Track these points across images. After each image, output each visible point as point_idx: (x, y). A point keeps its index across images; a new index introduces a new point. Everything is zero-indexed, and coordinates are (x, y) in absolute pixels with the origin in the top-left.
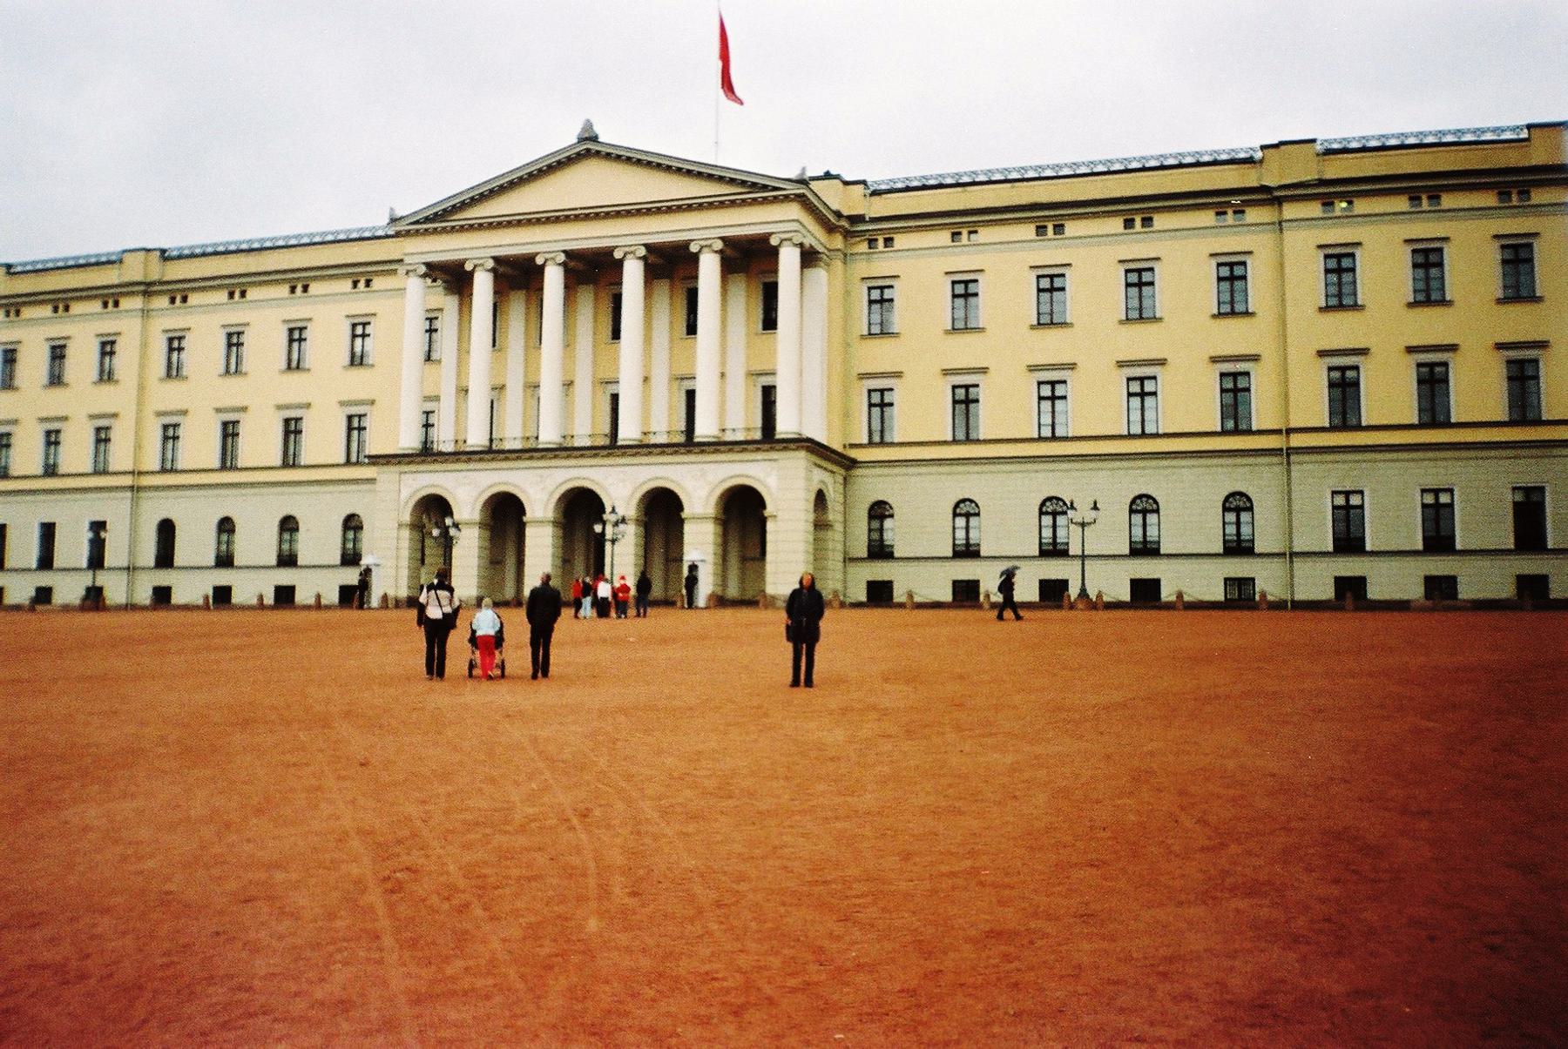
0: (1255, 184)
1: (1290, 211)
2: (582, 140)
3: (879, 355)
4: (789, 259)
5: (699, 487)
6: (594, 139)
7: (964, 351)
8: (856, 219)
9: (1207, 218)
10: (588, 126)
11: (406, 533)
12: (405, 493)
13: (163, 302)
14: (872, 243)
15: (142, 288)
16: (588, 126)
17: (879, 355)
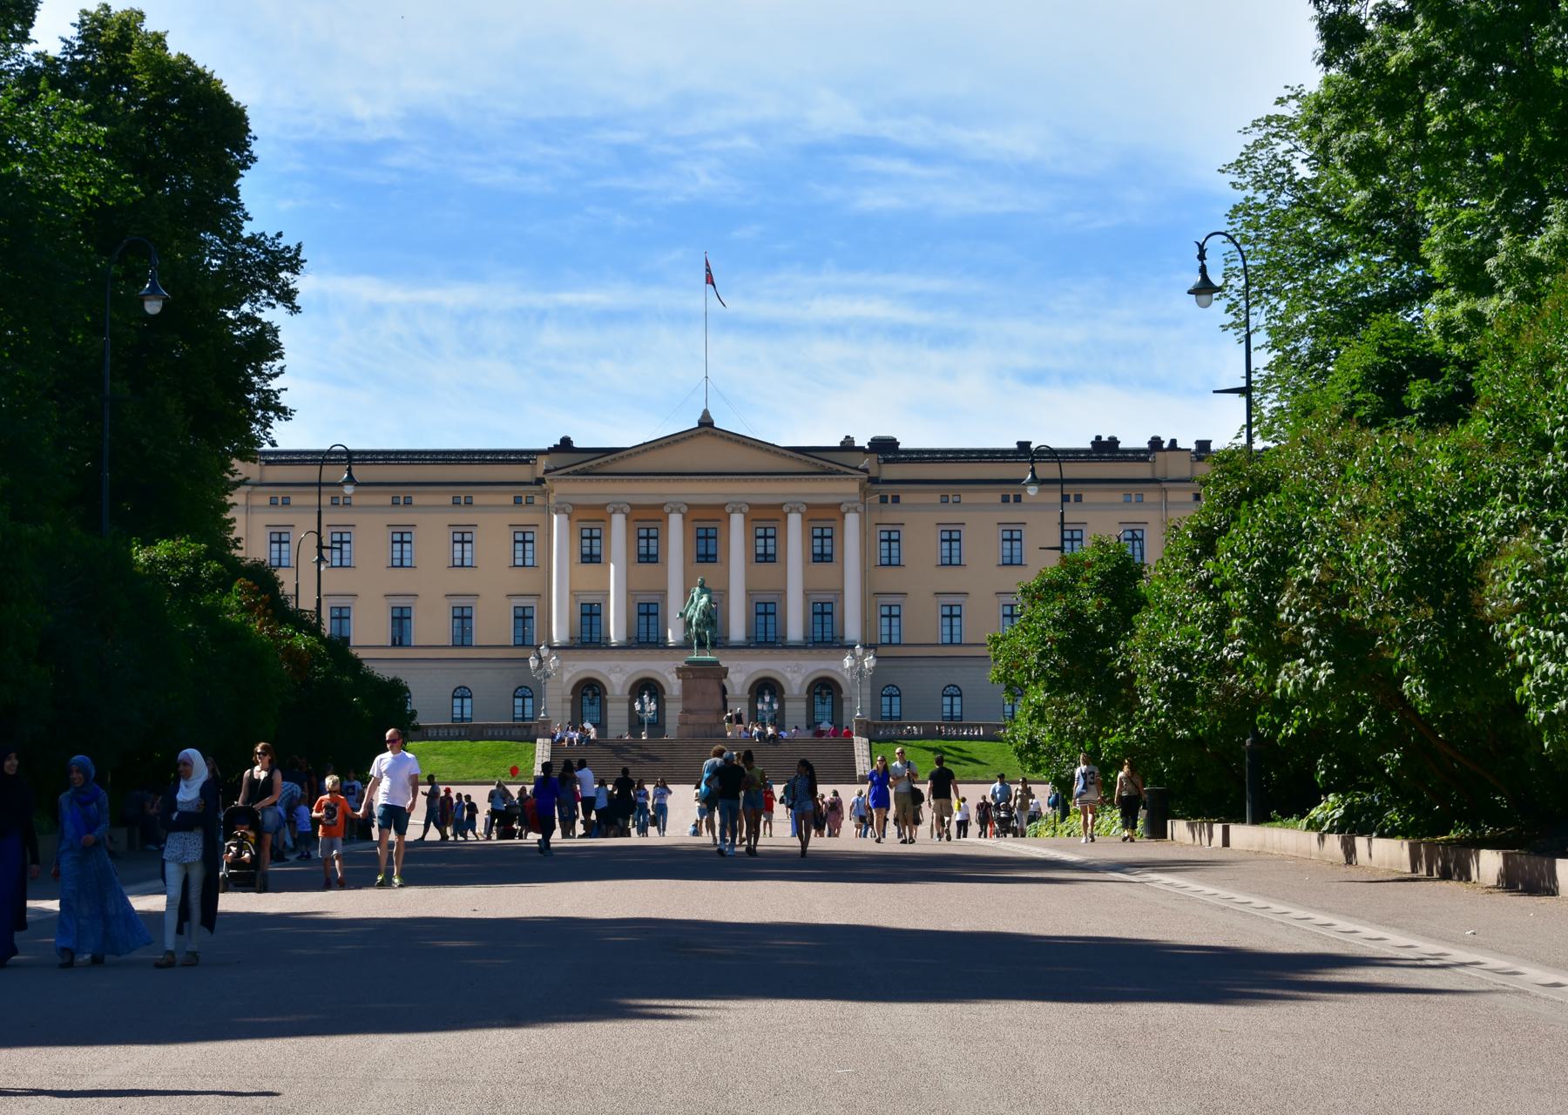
0: (1149, 476)
1: (1172, 496)
2: (701, 424)
3: (889, 579)
4: (852, 522)
5: (795, 673)
6: (711, 424)
7: (951, 579)
8: (874, 480)
9: (1118, 497)
10: (706, 413)
11: (568, 706)
12: (566, 676)
13: (266, 501)
14: (884, 500)
15: (248, 488)
16: (706, 413)
17: (889, 579)
